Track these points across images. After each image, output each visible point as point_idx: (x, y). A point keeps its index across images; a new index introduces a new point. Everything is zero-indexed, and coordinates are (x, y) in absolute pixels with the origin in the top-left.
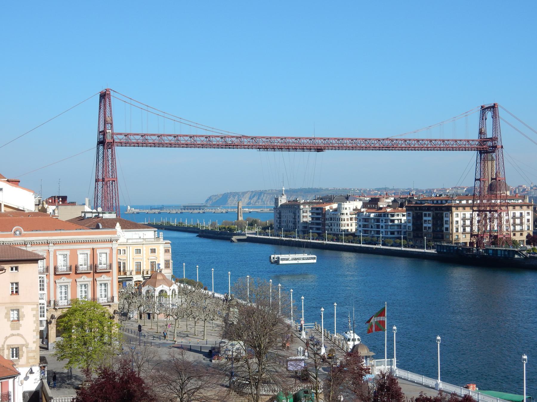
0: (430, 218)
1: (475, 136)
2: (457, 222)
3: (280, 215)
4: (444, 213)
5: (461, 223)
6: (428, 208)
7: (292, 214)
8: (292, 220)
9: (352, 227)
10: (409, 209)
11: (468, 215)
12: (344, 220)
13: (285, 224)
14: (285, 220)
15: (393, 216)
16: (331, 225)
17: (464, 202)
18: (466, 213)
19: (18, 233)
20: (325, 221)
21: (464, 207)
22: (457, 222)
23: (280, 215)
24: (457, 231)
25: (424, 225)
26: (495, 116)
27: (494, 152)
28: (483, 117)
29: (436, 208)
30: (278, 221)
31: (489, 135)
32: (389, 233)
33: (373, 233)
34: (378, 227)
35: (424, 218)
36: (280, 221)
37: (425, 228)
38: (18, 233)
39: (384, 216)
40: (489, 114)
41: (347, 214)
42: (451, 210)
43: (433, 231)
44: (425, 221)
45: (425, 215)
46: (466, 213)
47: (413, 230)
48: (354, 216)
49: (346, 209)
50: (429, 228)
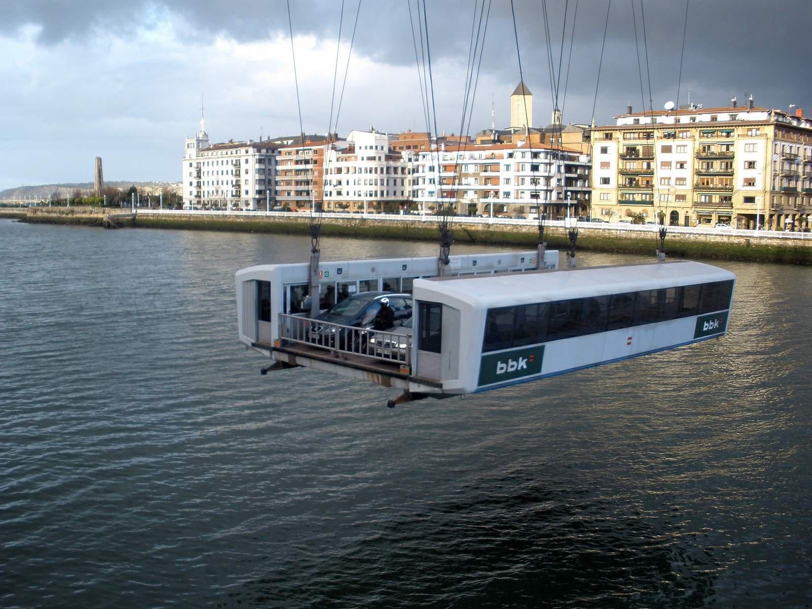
0: (688, 156)
3: (199, 172)
7: (231, 168)
8: (231, 178)
12: (376, 172)
13: (211, 188)
14: (211, 178)
16: (340, 183)
20: (321, 174)
23: (199, 172)
25: (660, 173)
30: (195, 184)
32: (527, 195)
35: (660, 157)
36: (198, 183)
41: (380, 159)
43: (696, 188)
45: (667, 149)
47: (620, 187)
48: (392, 164)
49: (376, 148)
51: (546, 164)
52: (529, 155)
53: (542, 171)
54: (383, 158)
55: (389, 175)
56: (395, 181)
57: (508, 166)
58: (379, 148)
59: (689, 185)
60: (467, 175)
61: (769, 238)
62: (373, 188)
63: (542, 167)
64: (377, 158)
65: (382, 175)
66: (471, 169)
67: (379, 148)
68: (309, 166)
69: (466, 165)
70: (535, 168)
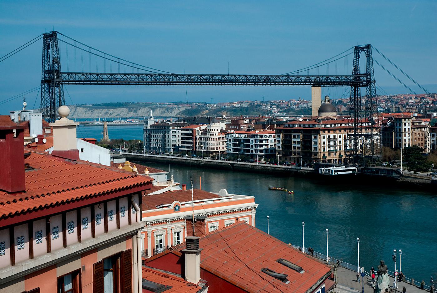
1: (350, 72)
2: (324, 142)
4: (313, 137)
5: (327, 143)
6: (298, 131)
9: (222, 147)
10: (278, 131)
11: (332, 137)
12: (214, 140)
15: (261, 137)
17: (328, 126)
18: (331, 135)
19: (177, 208)
21: (329, 131)
22: (324, 142)
24: (324, 151)
26: (368, 56)
27: (367, 86)
28: (357, 57)
29: (304, 132)
31: (363, 70)
33: (242, 151)
34: (248, 146)
37: (295, 148)
38: (177, 208)
39: (254, 137)
40: (363, 54)
41: (215, 134)
42: (320, 133)
44: (294, 142)
46: (331, 135)
48: (221, 136)
49: (215, 130)
50: (298, 148)
51: (266, 140)
52: (259, 137)
53: (264, 143)
54: (217, 134)
55: (219, 141)
56: (223, 143)
57: (252, 141)
58: (216, 130)
59: (300, 150)
60: (240, 143)
61: (304, 170)
62: (213, 147)
63: (264, 141)
64: (214, 135)
65: (216, 141)
66: (242, 141)
67: (216, 130)
68: (191, 136)
69: (241, 139)
70: (261, 141)
